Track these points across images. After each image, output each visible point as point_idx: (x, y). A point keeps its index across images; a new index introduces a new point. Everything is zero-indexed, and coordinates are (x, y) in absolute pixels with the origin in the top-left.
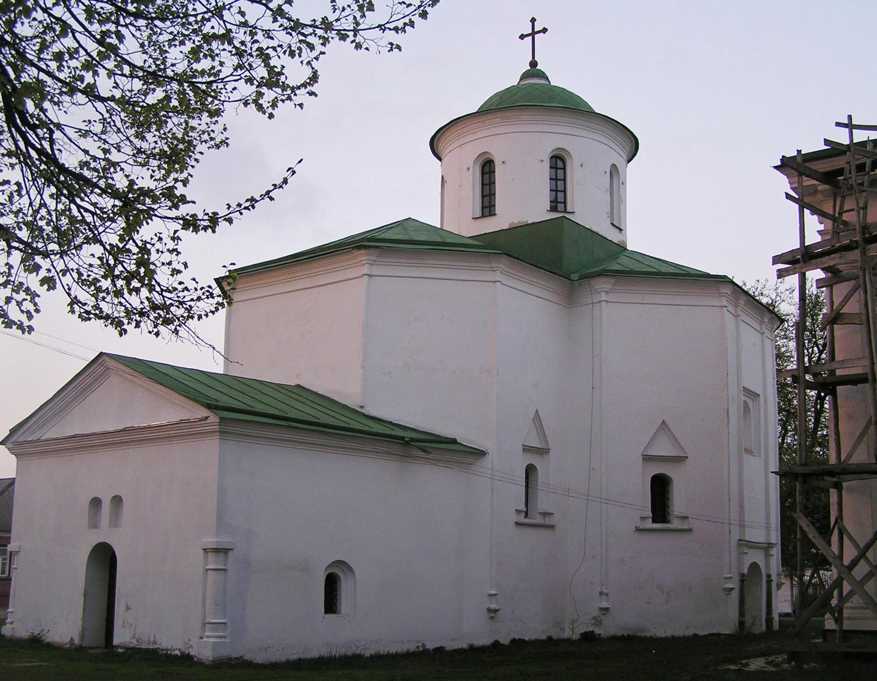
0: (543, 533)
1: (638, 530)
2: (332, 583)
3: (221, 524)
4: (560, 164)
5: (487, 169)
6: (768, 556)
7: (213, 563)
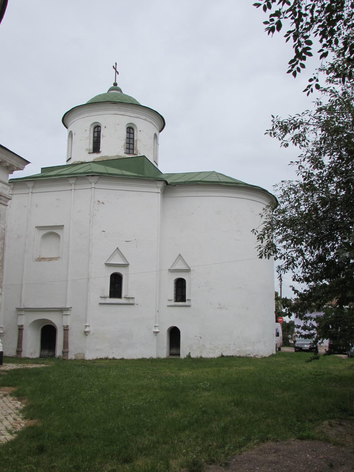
5: (96, 130)
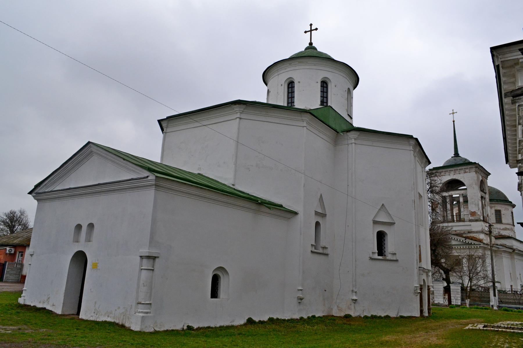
0: (322, 257)
1: (372, 259)
2: (216, 280)
3: (152, 241)
4: (325, 85)
5: (290, 86)
6: (427, 276)
7: (146, 265)
